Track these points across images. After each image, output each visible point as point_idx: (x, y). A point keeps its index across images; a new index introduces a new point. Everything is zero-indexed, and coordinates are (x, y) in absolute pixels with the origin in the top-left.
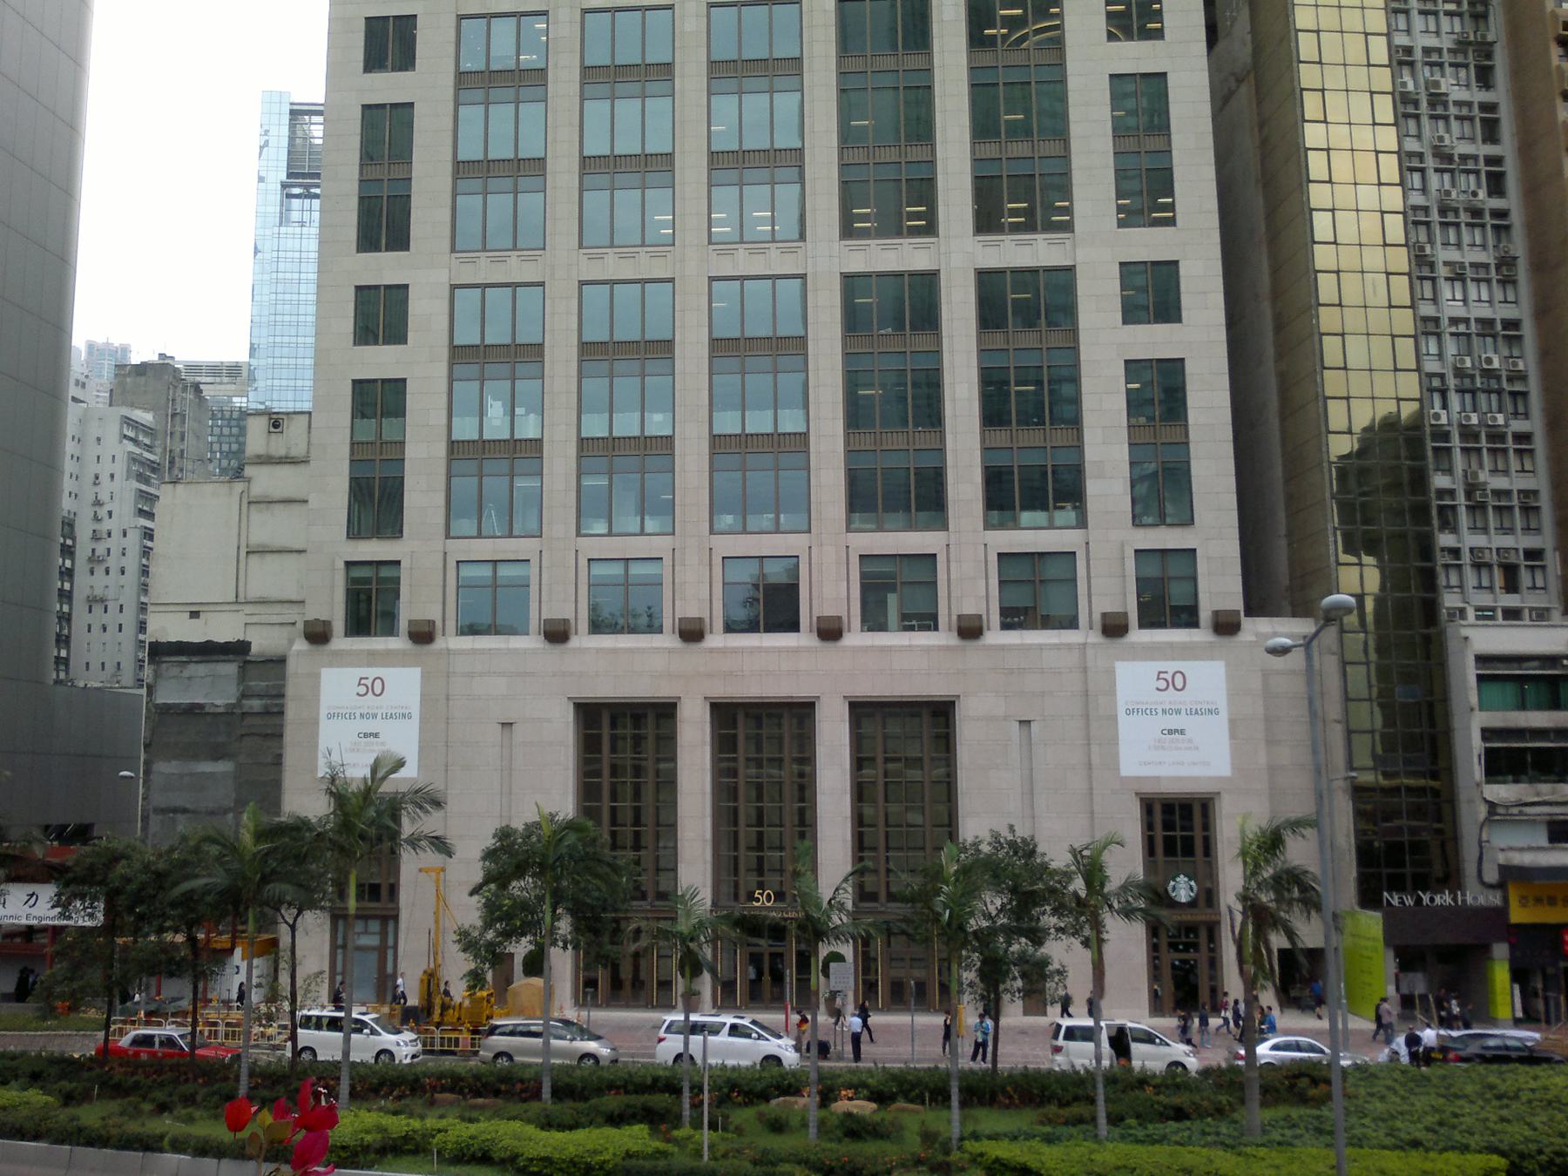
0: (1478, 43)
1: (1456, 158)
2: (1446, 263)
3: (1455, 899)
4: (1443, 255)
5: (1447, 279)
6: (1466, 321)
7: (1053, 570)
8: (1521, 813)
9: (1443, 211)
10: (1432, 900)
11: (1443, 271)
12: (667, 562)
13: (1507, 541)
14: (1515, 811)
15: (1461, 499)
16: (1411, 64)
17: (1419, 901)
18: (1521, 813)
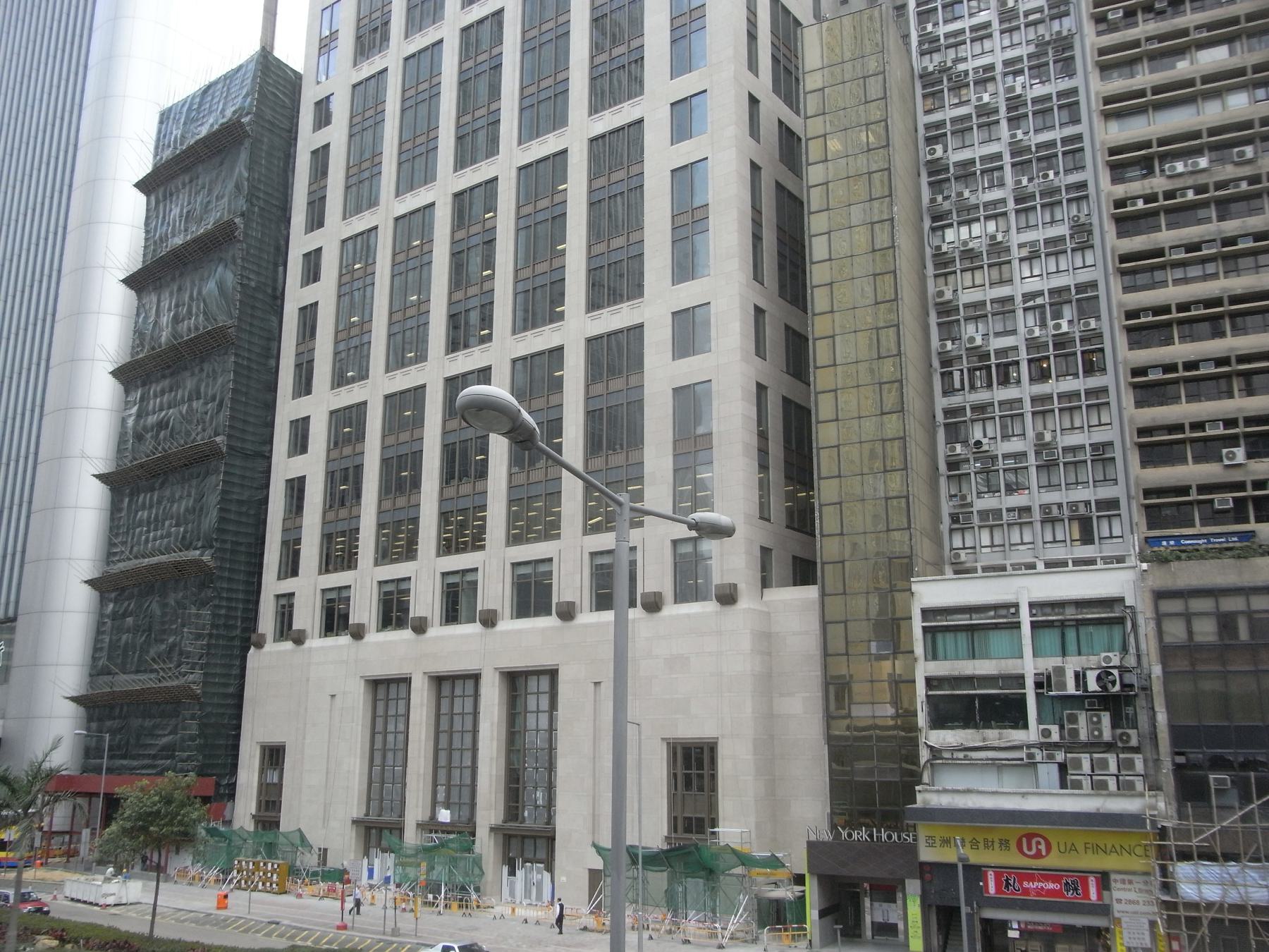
0: (1055, 41)
1: (1033, 149)
2: (1021, 246)
3: (871, 836)
4: (1016, 239)
5: (1021, 260)
6: (1041, 293)
8: (966, 758)
9: (1017, 201)
10: (850, 835)
11: (1016, 253)
13: (1081, 494)
14: (961, 755)
15: (1032, 460)
16: (993, 79)
18: (966, 758)
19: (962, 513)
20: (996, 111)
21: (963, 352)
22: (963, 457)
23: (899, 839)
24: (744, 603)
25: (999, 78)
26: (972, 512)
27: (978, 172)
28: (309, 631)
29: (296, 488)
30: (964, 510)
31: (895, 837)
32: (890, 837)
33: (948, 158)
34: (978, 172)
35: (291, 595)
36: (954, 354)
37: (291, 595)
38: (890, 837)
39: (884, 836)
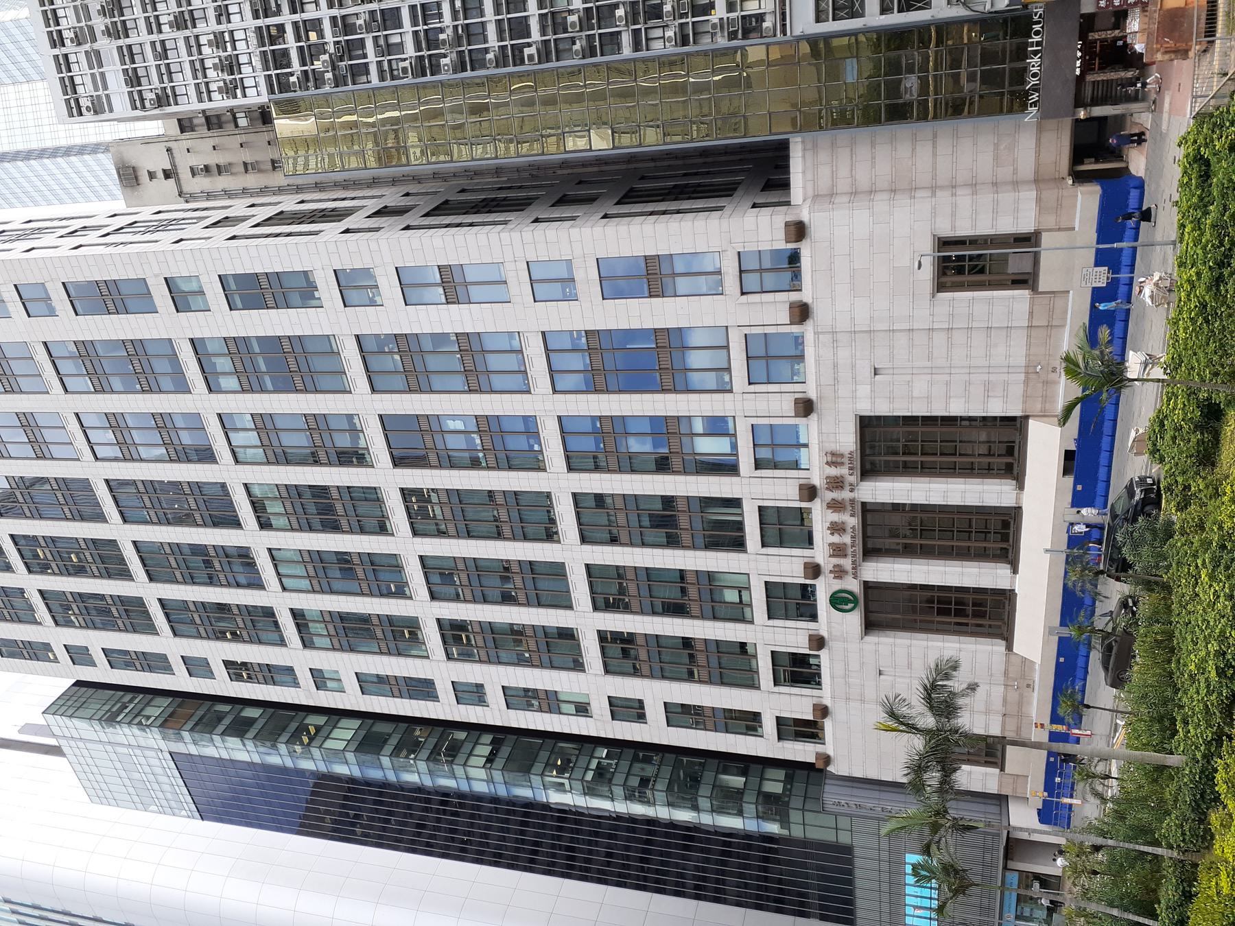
3: (1035, 53)
7: (758, 350)
10: (1034, 75)
12: (747, 331)
16: (344, 17)
17: (1035, 89)
19: (728, 29)
20: (372, 13)
21: (584, 34)
22: (677, 29)
23: (1039, 23)
24: (805, 216)
25: (344, 12)
26: (728, 18)
27: (425, 27)
28: (816, 701)
29: (679, 714)
30: (726, 27)
31: (1037, 27)
32: (1037, 33)
33: (411, 57)
34: (425, 27)
35: (780, 721)
36: (584, 42)
37: (780, 721)
38: (1037, 33)
39: (1037, 39)
